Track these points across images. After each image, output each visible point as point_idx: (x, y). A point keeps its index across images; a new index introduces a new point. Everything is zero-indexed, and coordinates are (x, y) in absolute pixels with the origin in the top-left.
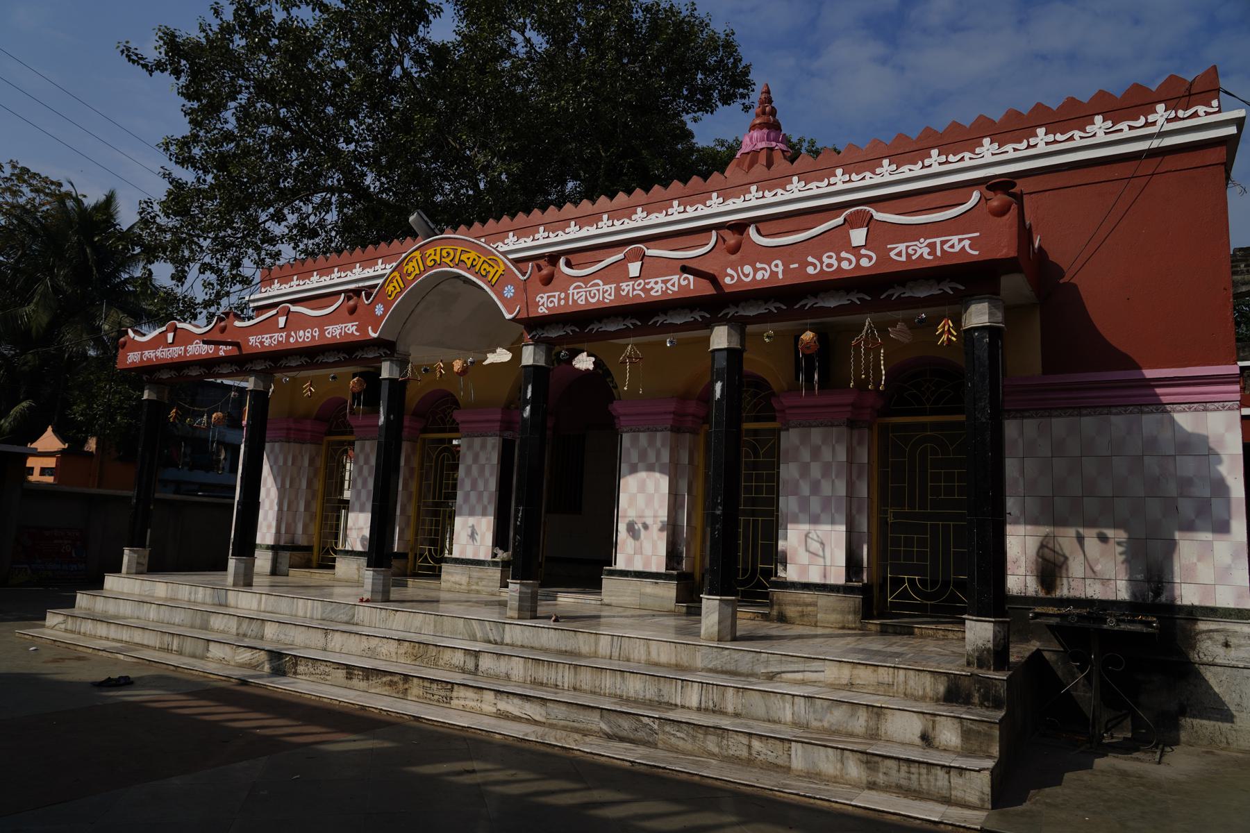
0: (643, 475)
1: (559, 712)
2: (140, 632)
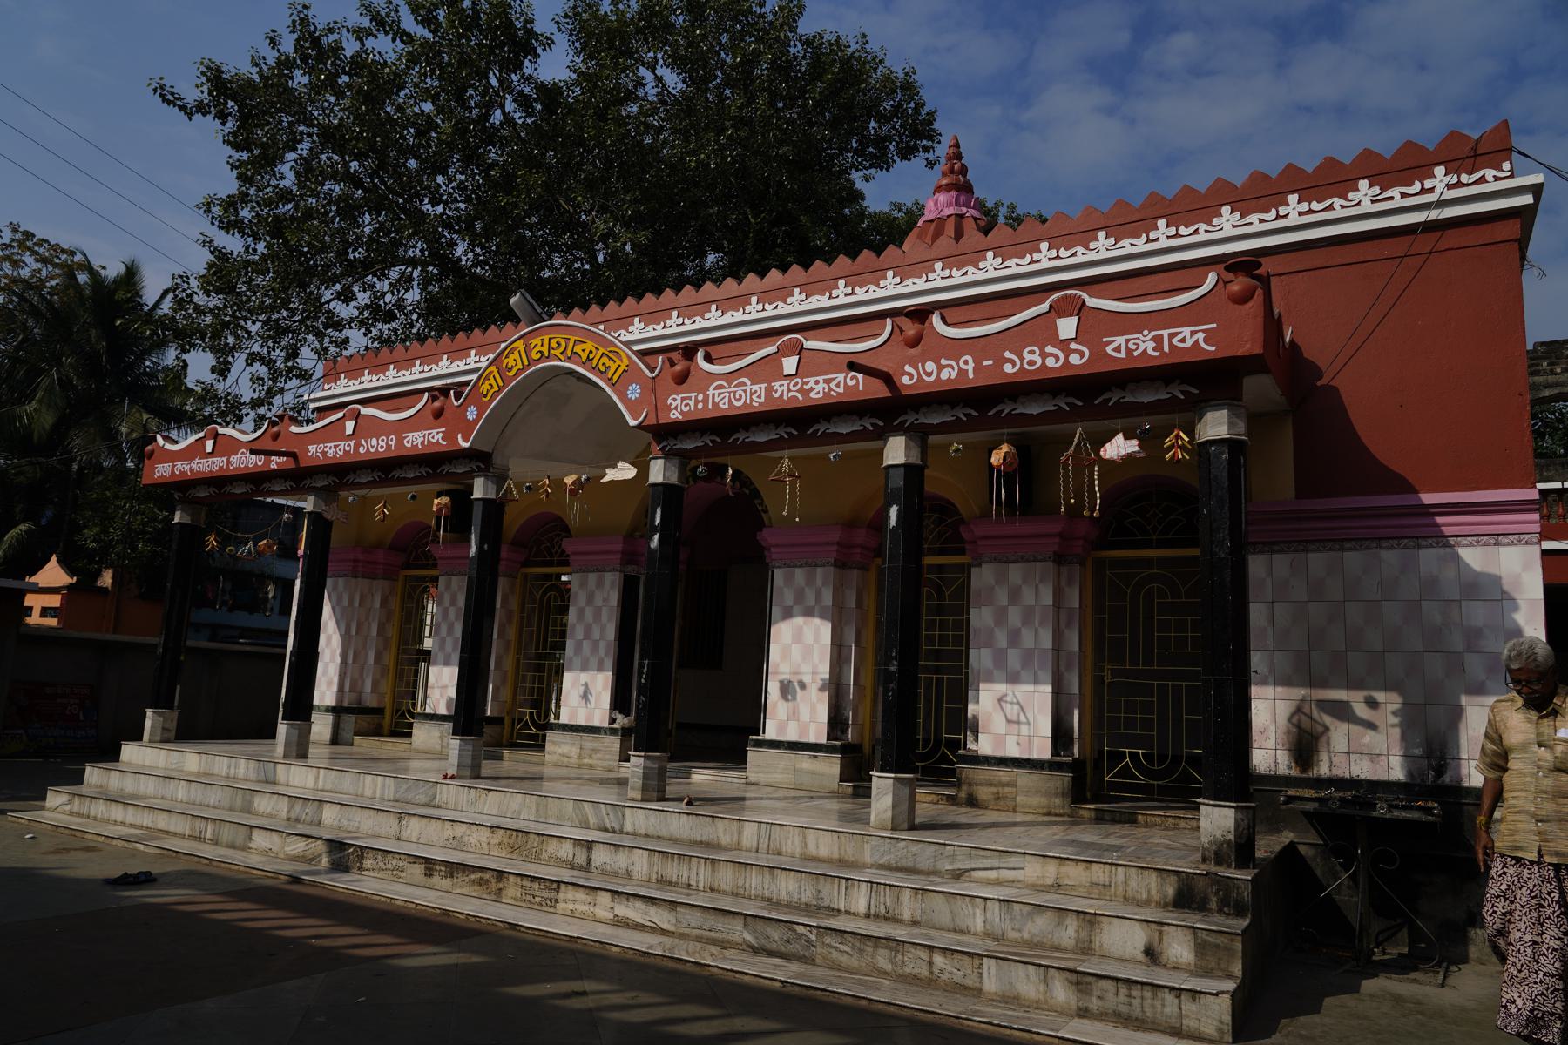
0: (799, 621)
1: (693, 919)
2: (165, 815)
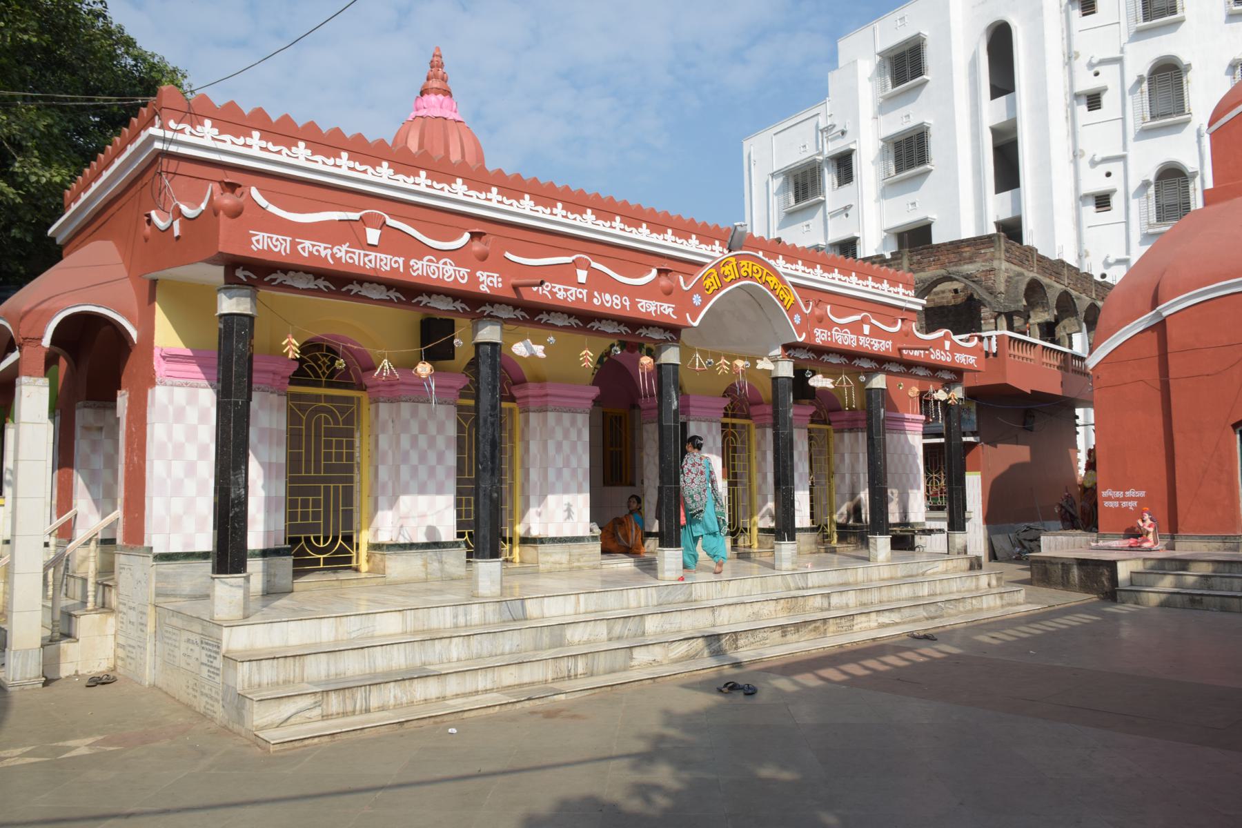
1: (906, 612)
2: (513, 669)
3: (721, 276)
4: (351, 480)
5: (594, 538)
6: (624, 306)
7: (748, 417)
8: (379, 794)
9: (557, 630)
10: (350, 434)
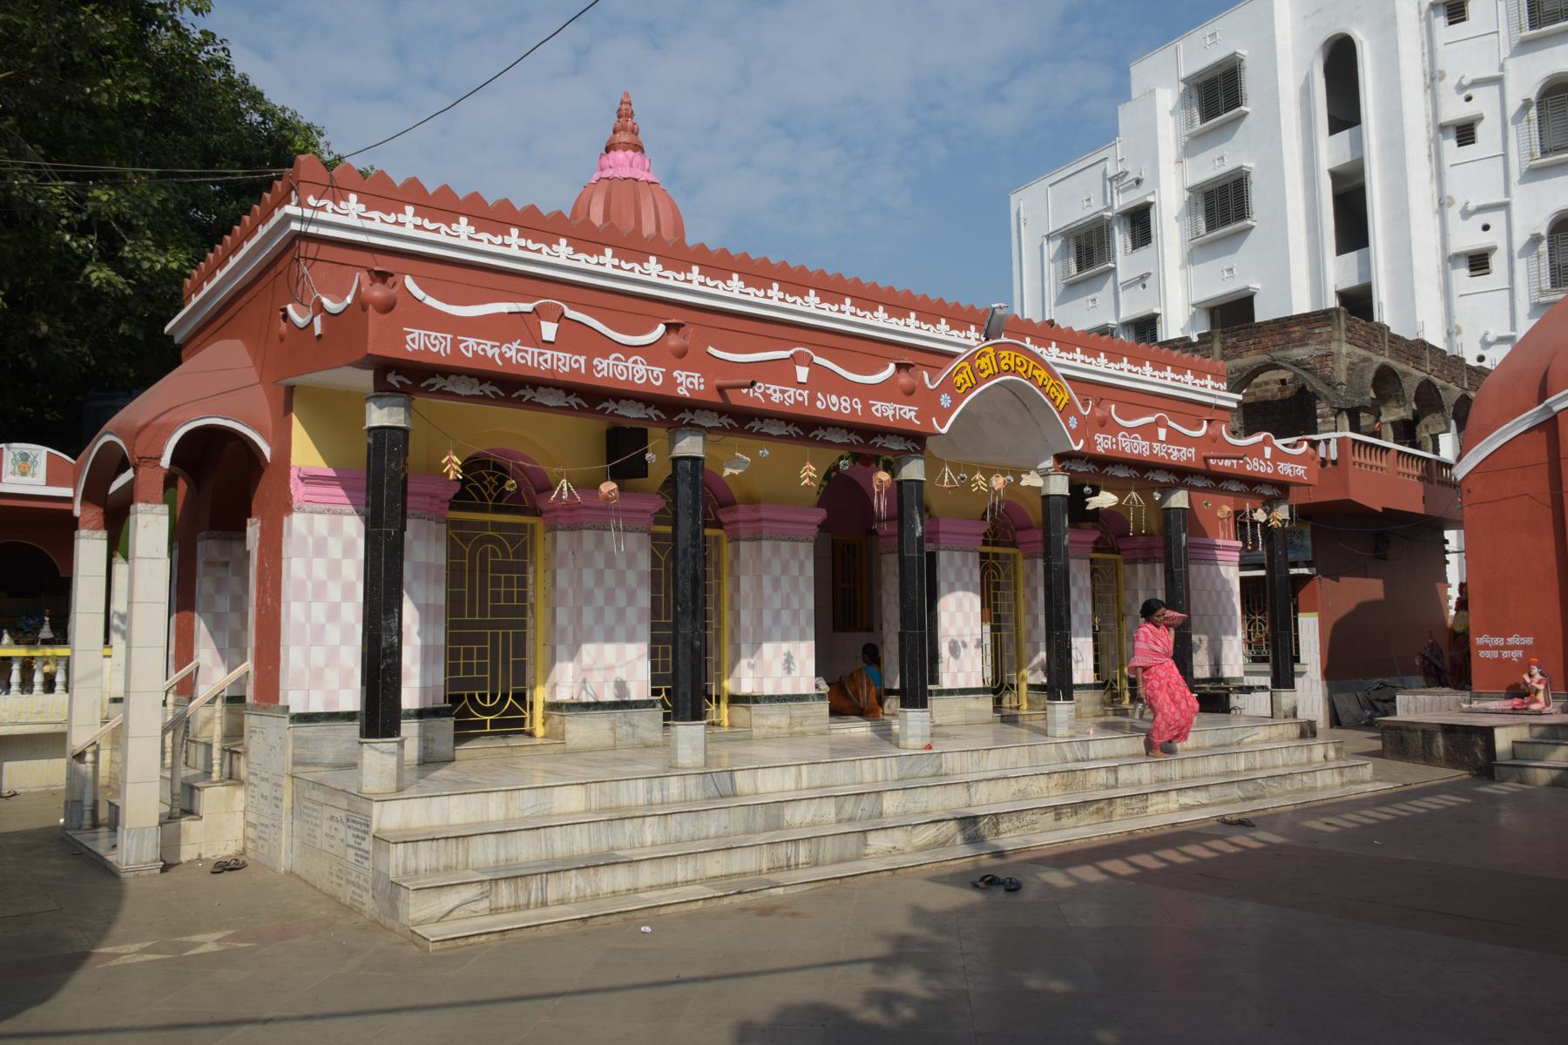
0: (960, 594)
1: (1216, 792)
2: (720, 856)
3: (976, 371)
4: (523, 625)
5: (821, 697)
6: (854, 410)
7: (1014, 545)
8: (558, 1001)
9: (773, 810)
10: (522, 569)
